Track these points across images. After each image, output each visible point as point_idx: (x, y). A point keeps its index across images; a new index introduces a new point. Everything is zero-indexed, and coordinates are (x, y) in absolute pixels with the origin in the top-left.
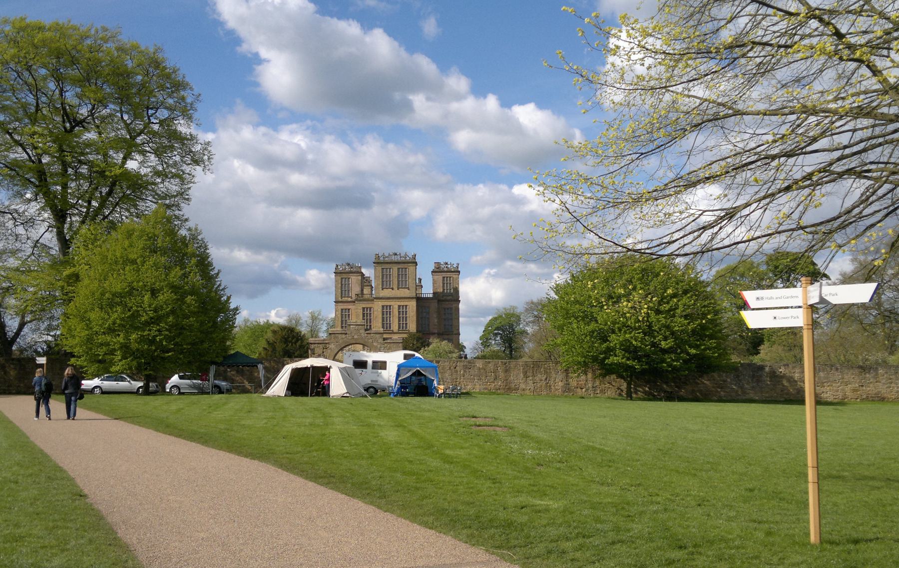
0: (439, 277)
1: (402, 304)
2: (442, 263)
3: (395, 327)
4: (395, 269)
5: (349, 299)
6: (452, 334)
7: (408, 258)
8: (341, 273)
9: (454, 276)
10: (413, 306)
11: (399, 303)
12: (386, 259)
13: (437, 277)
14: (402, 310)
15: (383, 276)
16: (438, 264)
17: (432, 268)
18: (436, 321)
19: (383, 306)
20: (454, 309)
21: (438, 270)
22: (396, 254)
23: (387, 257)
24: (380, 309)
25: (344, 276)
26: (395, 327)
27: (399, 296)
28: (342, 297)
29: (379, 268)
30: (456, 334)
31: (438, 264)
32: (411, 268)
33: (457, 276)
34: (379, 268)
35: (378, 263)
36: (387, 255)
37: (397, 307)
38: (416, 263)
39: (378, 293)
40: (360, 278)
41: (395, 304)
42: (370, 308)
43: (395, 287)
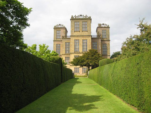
0: (100, 30)
1: (84, 39)
2: (102, 24)
5: (60, 40)
7: (87, 17)
8: (57, 28)
9: (107, 29)
11: (83, 39)
12: (77, 18)
13: (100, 30)
16: (100, 25)
17: (97, 26)
21: (100, 27)
22: (81, 16)
23: (77, 17)
24: (73, 41)
26: (81, 50)
27: (83, 35)
28: (57, 39)
29: (73, 22)
30: (109, 56)
31: (100, 25)
33: (109, 30)
34: (73, 22)
35: (73, 19)
36: (77, 16)
37: (82, 40)
38: (91, 19)
39: (73, 34)
40: (65, 30)
41: (81, 39)
42: (69, 42)
43: (81, 31)
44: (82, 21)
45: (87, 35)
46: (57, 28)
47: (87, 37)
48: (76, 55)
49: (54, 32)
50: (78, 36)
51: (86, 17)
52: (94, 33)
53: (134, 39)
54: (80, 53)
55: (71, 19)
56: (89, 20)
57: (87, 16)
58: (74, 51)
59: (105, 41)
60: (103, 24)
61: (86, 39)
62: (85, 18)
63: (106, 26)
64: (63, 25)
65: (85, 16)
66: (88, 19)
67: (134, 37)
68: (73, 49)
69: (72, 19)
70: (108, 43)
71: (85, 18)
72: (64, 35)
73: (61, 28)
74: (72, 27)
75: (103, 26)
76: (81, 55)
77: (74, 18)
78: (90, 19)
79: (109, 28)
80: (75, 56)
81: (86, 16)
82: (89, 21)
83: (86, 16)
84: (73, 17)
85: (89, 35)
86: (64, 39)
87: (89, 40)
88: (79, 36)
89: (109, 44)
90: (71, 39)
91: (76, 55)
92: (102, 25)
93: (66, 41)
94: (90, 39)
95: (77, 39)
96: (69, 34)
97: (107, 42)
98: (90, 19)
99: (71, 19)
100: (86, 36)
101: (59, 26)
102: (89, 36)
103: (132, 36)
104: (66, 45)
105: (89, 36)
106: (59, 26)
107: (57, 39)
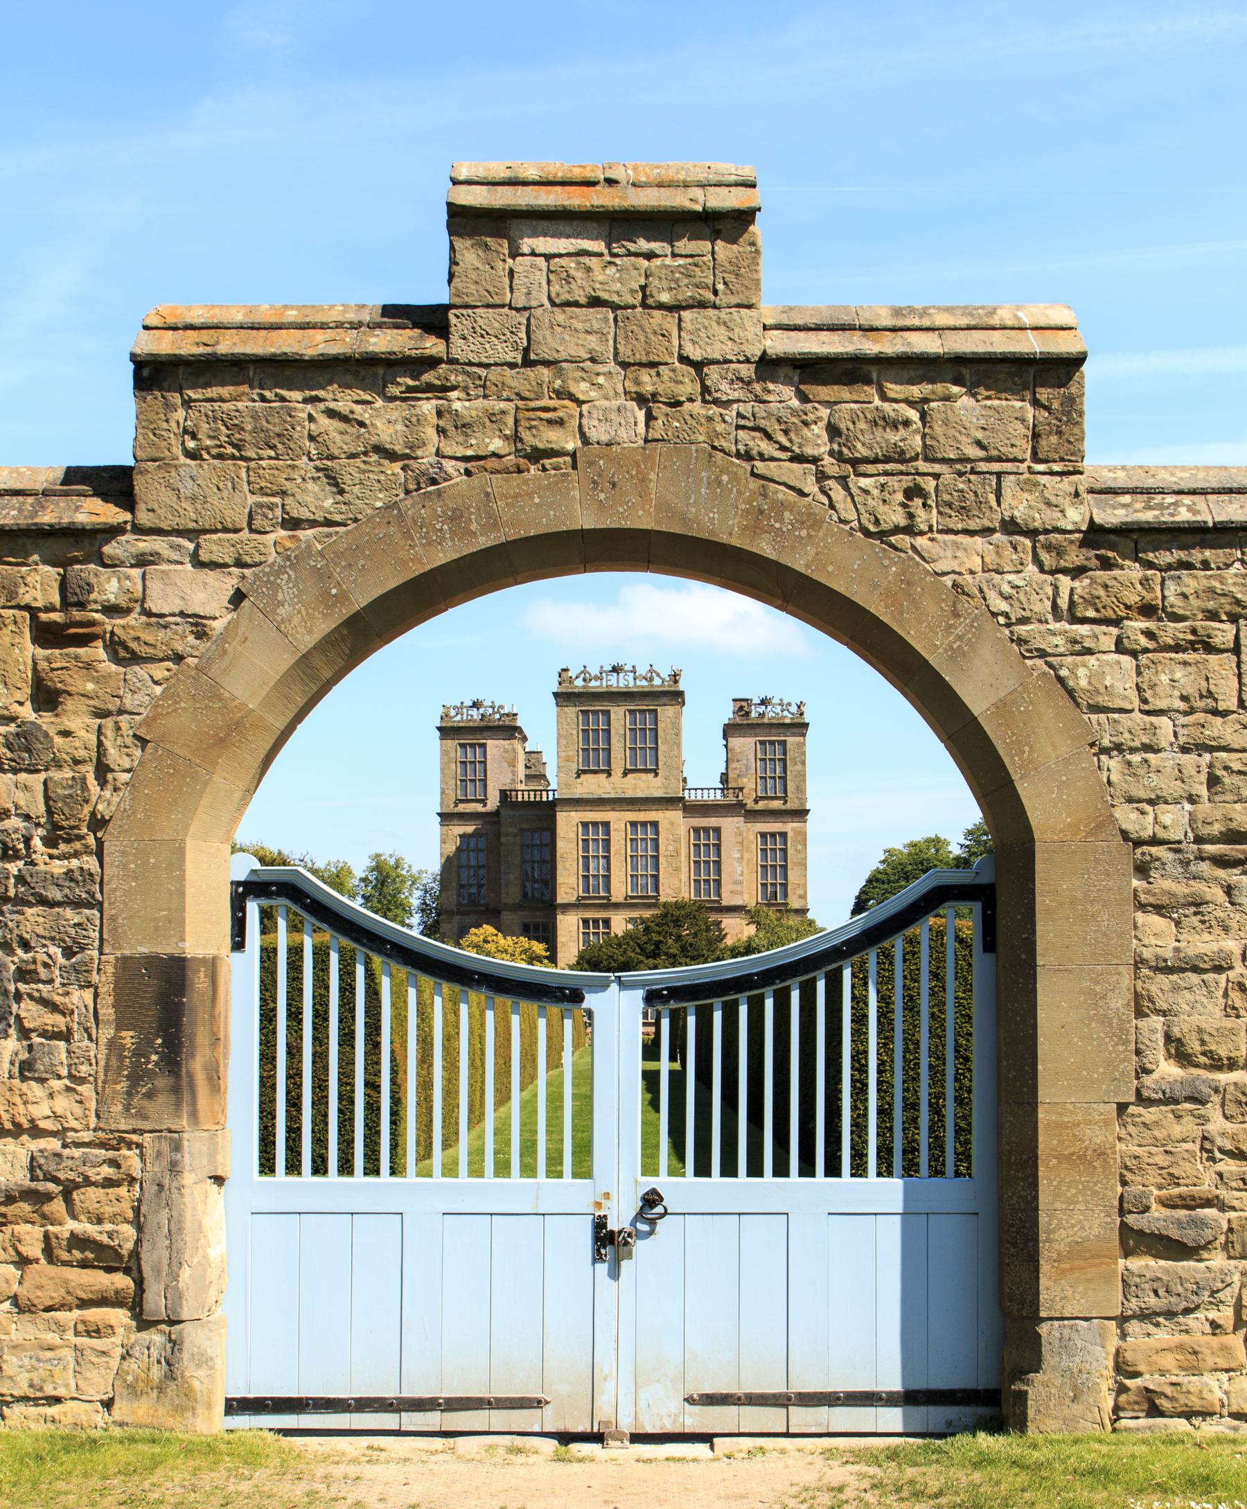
4: (618, 714)
7: (657, 682)
12: (593, 683)
16: (742, 706)
17: (726, 713)
20: (790, 835)
23: (596, 678)
31: (742, 706)
34: (571, 711)
36: (594, 671)
41: (618, 820)
51: (651, 679)
54: (617, 906)
57: (658, 675)
62: (644, 683)
63: (786, 713)
64: (501, 707)
65: (642, 670)
70: (793, 829)
71: (644, 683)
74: (564, 742)
77: (579, 683)
79: (806, 725)
81: (651, 671)
83: (651, 671)
89: (802, 838)
97: (790, 827)
101: (475, 713)
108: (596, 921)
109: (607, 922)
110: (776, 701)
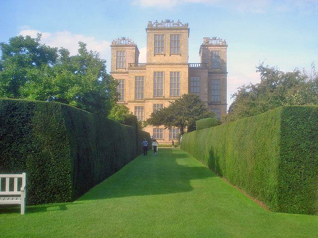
1: (175, 70)
3: (166, 93)
5: (124, 70)
6: (220, 104)
7: (181, 25)
8: (117, 46)
10: (185, 72)
11: (171, 70)
14: (175, 76)
15: (155, 42)
18: (206, 90)
19: (155, 73)
22: (168, 21)
23: (160, 24)
24: (152, 76)
25: (120, 49)
26: (166, 93)
27: (170, 62)
28: (117, 69)
29: (152, 35)
32: (184, 34)
35: (151, 29)
36: (160, 22)
37: (169, 73)
38: (189, 30)
43: (168, 55)
44: (171, 32)
45: (178, 62)
46: (117, 46)
47: (179, 66)
48: (157, 102)
49: (112, 54)
50: (161, 64)
51: (179, 24)
52: (195, 59)
53: (248, 90)
55: (147, 29)
56: (183, 31)
57: (181, 24)
58: (152, 95)
59: (216, 73)
60: (215, 39)
61: (178, 70)
65: (176, 22)
66: (183, 29)
67: (248, 87)
68: (152, 91)
69: (150, 29)
72: (133, 61)
73: (126, 46)
75: (214, 42)
76: (167, 105)
77: (154, 26)
78: (186, 28)
79: (227, 46)
80: (155, 105)
82: (183, 32)
84: (152, 24)
85: (184, 62)
86: (133, 69)
87: (184, 73)
88: (164, 64)
90: (147, 69)
91: (157, 102)
92: (211, 40)
93: (138, 73)
94: (186, 70)
95: (160, 70)
96: (142, 59)
98: (186, 28)
99: (147, 29)
100: (177, 64)
101: (122, 42)
102: (185, 64)
103: (246, 86)
104: (136, 82)
105: (185, 64)
106: (122, 42)
107: (117, 69)
108: (158, 105)
109: (162, 105)
110: (217, 38)
